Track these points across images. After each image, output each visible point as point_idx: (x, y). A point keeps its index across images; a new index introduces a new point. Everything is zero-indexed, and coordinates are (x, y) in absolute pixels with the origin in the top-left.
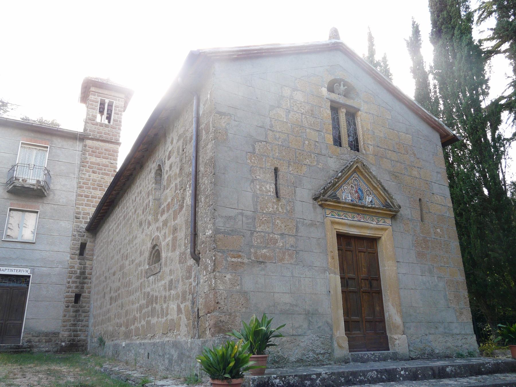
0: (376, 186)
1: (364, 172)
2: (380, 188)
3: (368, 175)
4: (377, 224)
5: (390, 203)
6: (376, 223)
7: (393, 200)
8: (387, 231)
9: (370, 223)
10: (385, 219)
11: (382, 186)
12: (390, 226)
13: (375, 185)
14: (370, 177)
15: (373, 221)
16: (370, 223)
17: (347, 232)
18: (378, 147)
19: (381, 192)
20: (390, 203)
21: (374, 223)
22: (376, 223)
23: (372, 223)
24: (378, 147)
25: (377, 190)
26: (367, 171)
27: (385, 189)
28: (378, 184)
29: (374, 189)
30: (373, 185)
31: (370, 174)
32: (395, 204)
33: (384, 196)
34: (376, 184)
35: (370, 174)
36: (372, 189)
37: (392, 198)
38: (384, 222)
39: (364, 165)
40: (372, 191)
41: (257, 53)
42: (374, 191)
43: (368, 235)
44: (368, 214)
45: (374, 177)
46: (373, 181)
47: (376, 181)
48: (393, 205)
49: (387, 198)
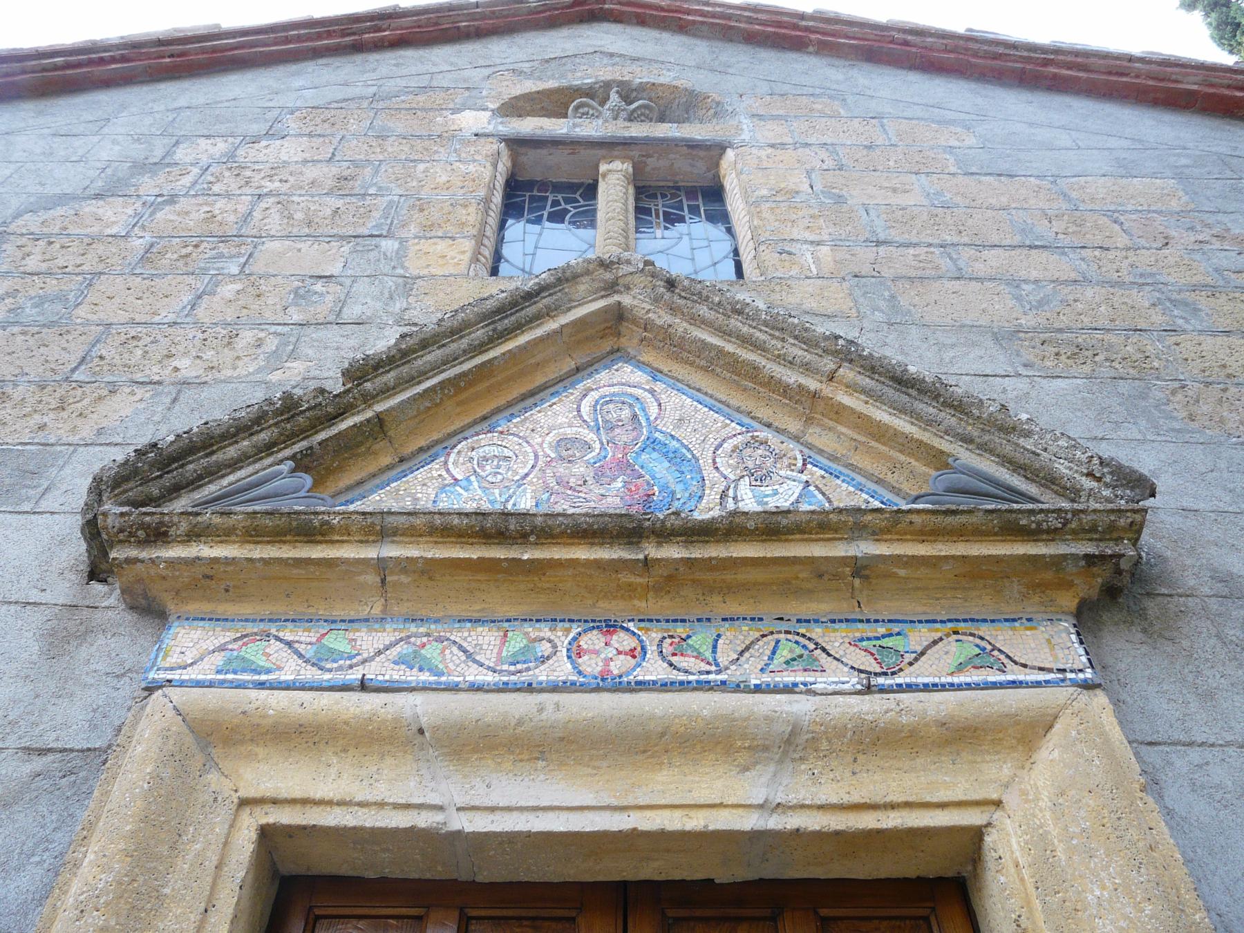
0: (812, 384)
1: (681, 326)
2: (852, 388)
3: (725, 333)
4: (868, 689)
5: (1004, 475)
6: (854, 681)
7: (1028, 444)
8: (1050, 752)
9: (758, 689)
10: (984, 630)
11: (872, 367)
12: (1087, 686)
13: (792, 377)
14: (746, 341)
15: (812, 666)
16: (758, 689)
17: (423, 820)
18: (879, 243)
19: (881, 415)
20: (1004, 475)
21: (821, 682)
22: (854, 681)
23: (789, 689)
24: (879, 243)
25: (839, 412)
26: (703, 310)
27: (903, 381)
28: (828, 364)
29: (809, 421)
30: (785, 390)
31: (735, 323)
32: (1062, 468)
33: (926, 437)
34: (807, 368)
35: (735, 323)
36: (794, 426)
37: (1009, 429)
38: (987, 656)
39: (671, 284)
40: (796, 439)
41: (68, 66)
42: (816, 436)
43: (749, 822)
44: (734, 608)
45: (778, 326)
46: (781, 359)
47: (797, 352)
48: (1050, 481)
49: (944, 445)
